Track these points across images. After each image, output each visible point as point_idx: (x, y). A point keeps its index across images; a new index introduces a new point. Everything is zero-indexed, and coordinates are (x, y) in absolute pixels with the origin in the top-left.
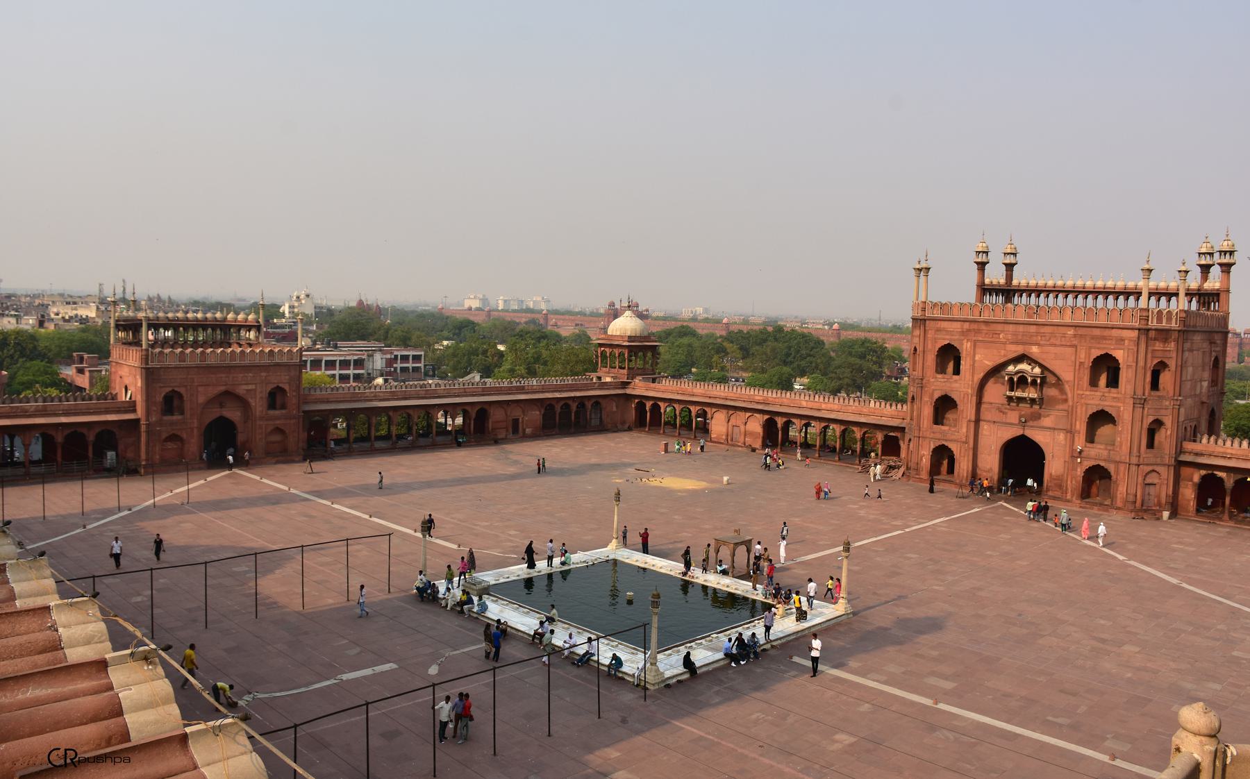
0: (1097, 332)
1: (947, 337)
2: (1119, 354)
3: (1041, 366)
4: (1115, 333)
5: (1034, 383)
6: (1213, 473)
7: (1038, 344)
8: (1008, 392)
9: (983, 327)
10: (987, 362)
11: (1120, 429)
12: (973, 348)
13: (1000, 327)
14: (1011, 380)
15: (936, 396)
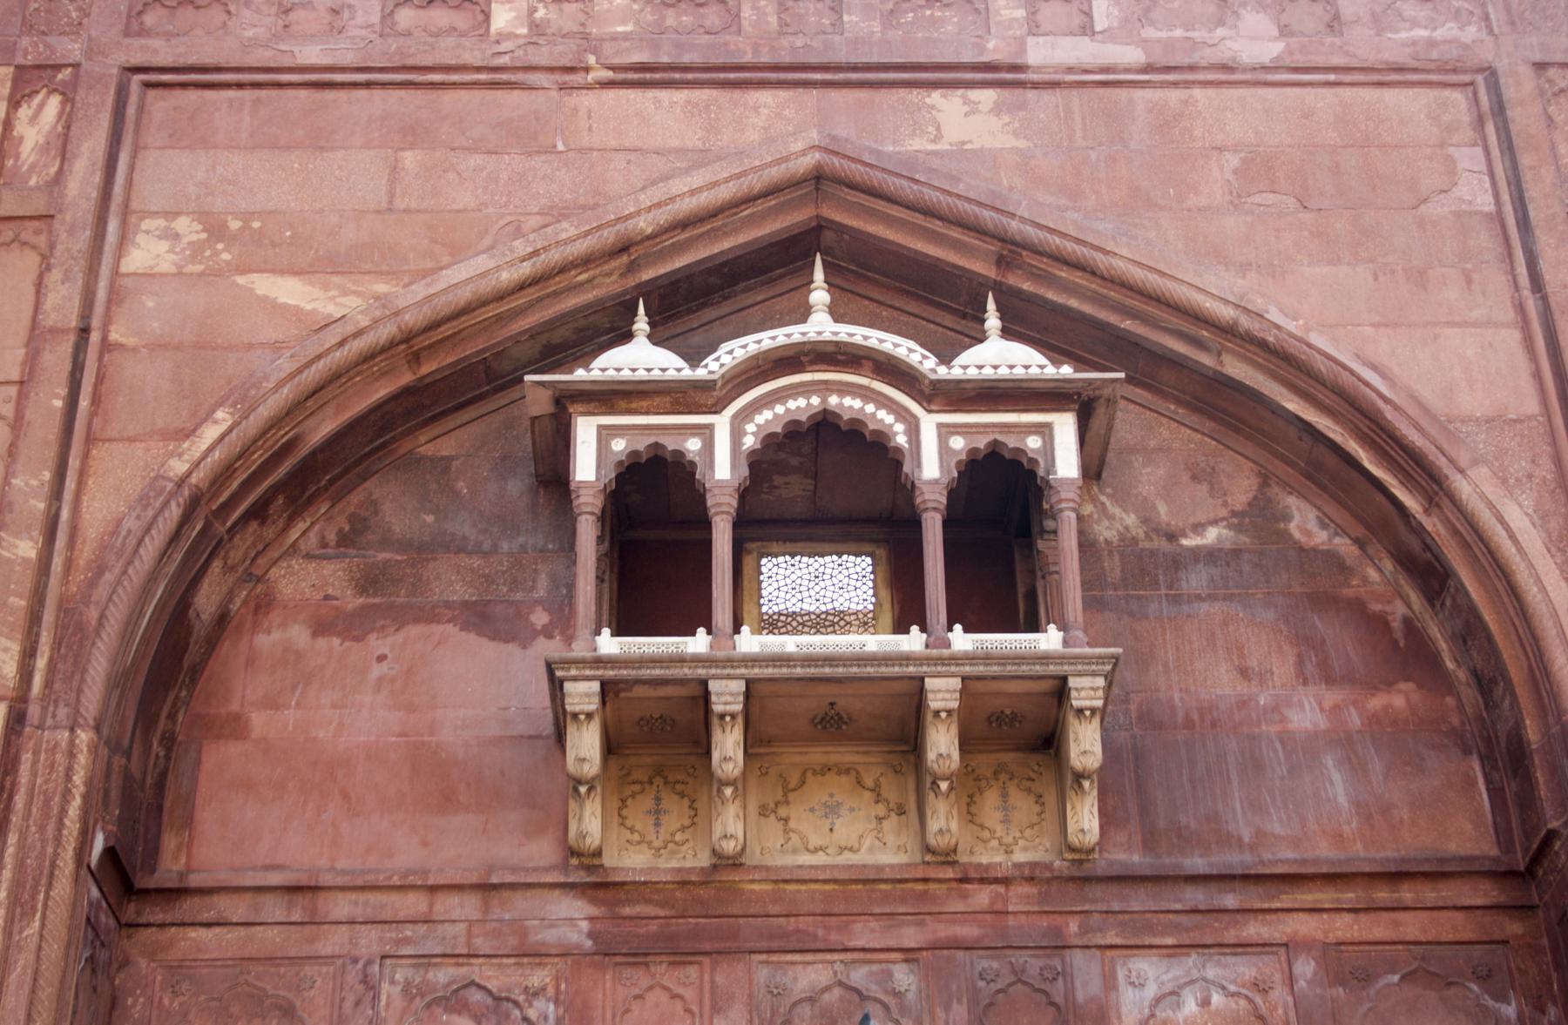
10: (290, 291)
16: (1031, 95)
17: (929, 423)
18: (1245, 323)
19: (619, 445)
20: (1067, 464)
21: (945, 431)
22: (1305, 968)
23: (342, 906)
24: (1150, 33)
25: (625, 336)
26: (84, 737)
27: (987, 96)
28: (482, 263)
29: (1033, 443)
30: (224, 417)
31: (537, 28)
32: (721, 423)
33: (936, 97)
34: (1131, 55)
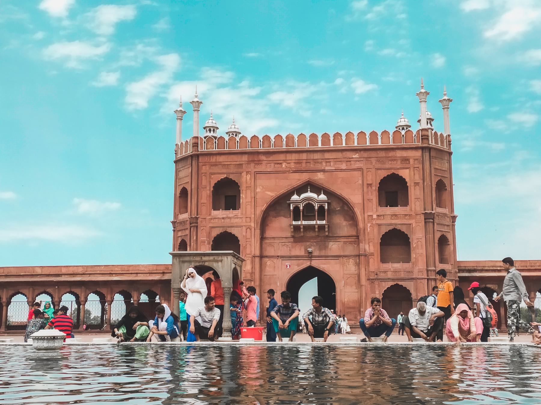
0: (382, 154)
1: (224, 171)
2: (405, 174)
3: (327, 192)
4: (399, 154)
5: (321, 208)
6: (486, 288)
7: (324, 171)
8: (294, 223)
9: (263, 158)
10: (269, 193)
11: (414, 246)
12: (253, 180)
13: (282, 157)
14: (297, 209)
15: (215, 233)
16: (325, 173)
17: (316, 204)
18: (340, 195)
19: (294, 206)
20: (326, 208)
21: (318, 204)
22: (342, 243)
23: (276, 239)
24: (336, 166)
25: (294, 194)
26: (259, 230)
27: (322, 173)
28: (283, 191)
29: (324, 205)
30: (265, 205)
31: (286, 166)
32: (301, 204)
33: (318, 173)
34: (334, 168)
